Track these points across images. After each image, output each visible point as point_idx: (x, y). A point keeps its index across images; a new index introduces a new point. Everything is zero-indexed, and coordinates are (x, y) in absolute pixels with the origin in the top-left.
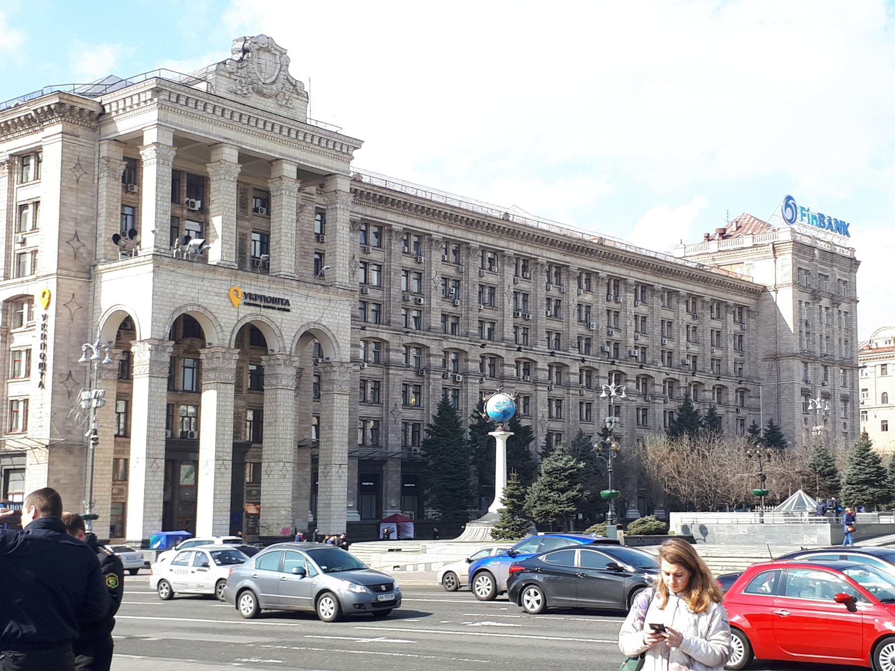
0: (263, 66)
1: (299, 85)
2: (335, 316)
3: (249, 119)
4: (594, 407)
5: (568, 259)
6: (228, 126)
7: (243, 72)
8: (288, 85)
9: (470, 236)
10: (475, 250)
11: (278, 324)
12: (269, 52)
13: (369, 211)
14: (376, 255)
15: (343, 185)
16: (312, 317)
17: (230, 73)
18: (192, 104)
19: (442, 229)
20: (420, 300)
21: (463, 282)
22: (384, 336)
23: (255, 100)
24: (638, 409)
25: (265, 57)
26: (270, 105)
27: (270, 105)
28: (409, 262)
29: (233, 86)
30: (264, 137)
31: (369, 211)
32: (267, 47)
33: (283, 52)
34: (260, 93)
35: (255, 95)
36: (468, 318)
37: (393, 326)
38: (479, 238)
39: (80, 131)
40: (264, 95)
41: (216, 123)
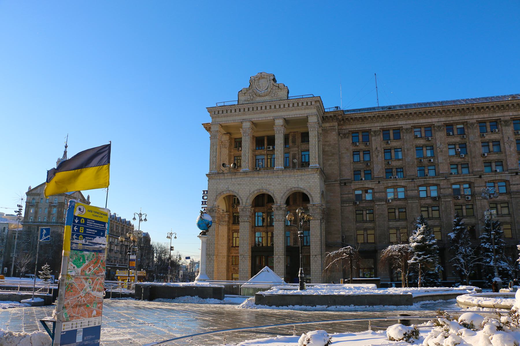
0: (261, 85)
1: (280, 85)
2: (310, 183)
7: (251, 91)
8: (274, 88)
9: (467, 117)
10: (472, 124)
11: (272, 192)
12: (264, 78)
13: (385, 124)
15: (313, 120)
16: (294, 185)
17: (245, 94)
18: (225, 112)
19: (443, 119)
20: (430, 160)
21: (467, 144)
23: (258, 99)
26: (267, 98)
27: (267, 98)
31: (385, 124)
34: (260, 96)
35: (258, 98)
36: (472, 163)
37: (407, 177)
38: (476, 117)
40: (262, 96)
41: (238, 115)
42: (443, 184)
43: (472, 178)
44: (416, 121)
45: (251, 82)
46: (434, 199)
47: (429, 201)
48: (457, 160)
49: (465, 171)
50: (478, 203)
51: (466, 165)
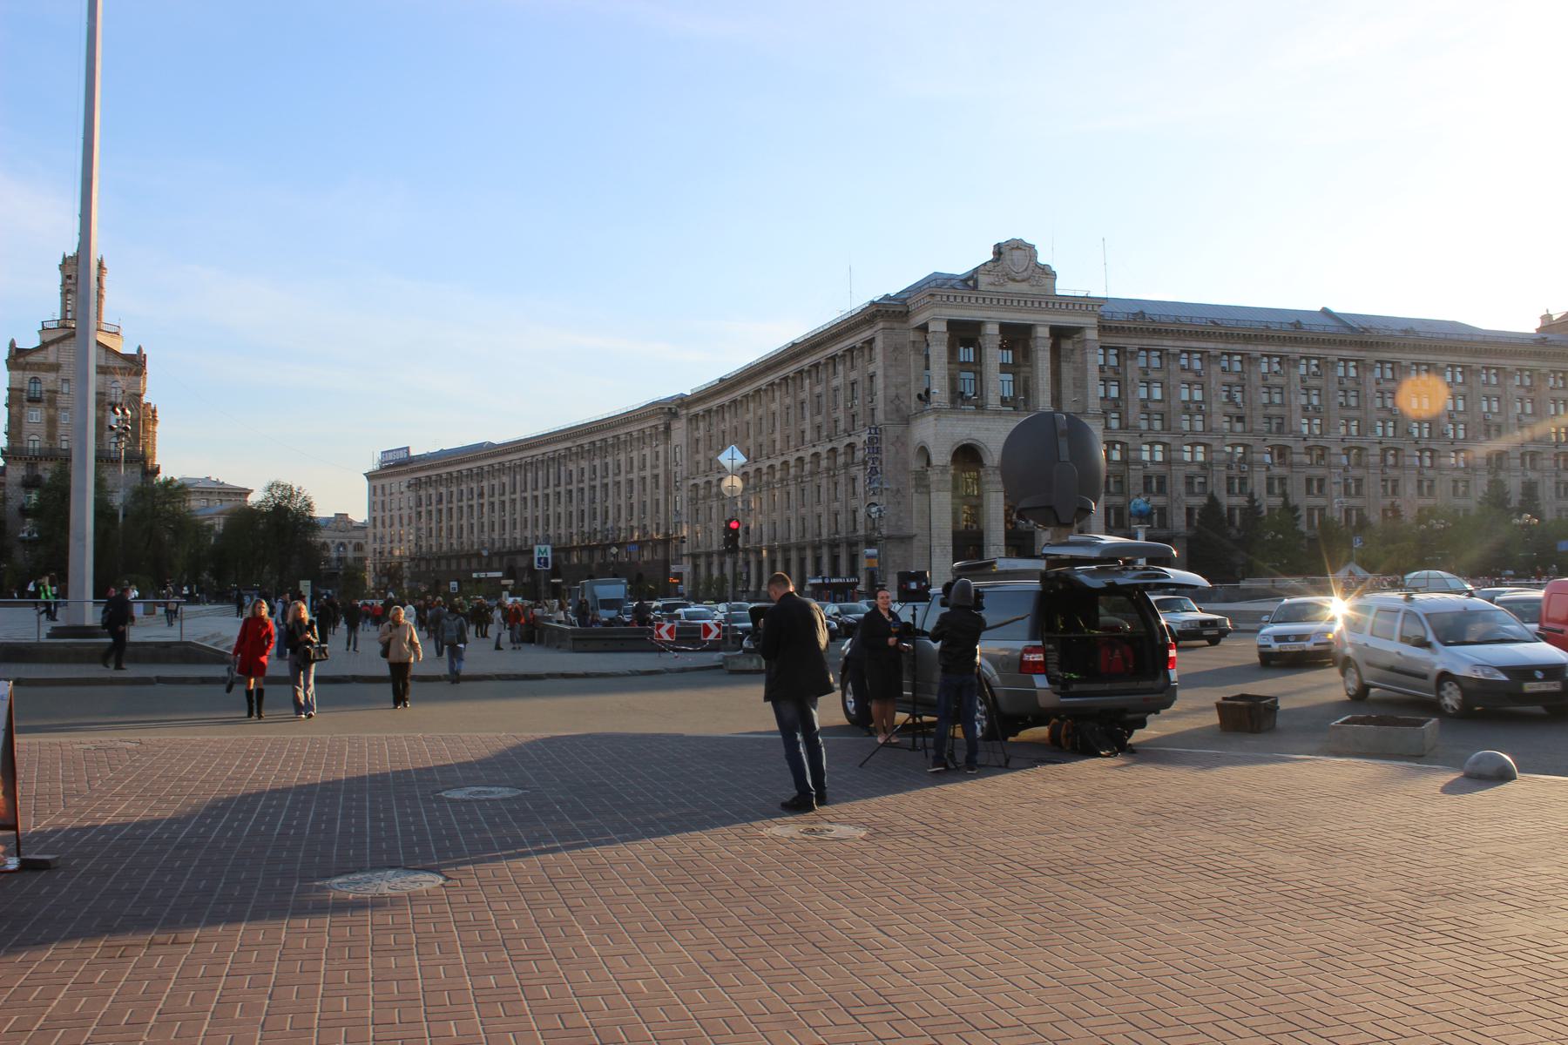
3: (1007, 301)
4: (1401, 483)
5: (1363, 354)
6: (989, 308)
9: (1250, 347)
14: (1153, 375)
15: (1092, 335)
19: (1221, 346)
22: (1166, 440)
24: (1455, 481)
25: (1017, 253)
26: (1024, 287)
27: (1024, 287)
28: (1190, 376)
29: (991, 279)
30: (1020, 311)
32: (1018, 246)
33: (1032, 247)
34: (1014, 280)
38: (1261, 348)
39: (896, 325)
42: (1216, 444)
43: (1247, 440)
44: (1187, 344)
45: (999, 250)
46: (1203, 465)
47: (1195, 469)
48: (1232, 410)
49: (1239, 427)
50: (1256, 476)
51: (1240, 419)
